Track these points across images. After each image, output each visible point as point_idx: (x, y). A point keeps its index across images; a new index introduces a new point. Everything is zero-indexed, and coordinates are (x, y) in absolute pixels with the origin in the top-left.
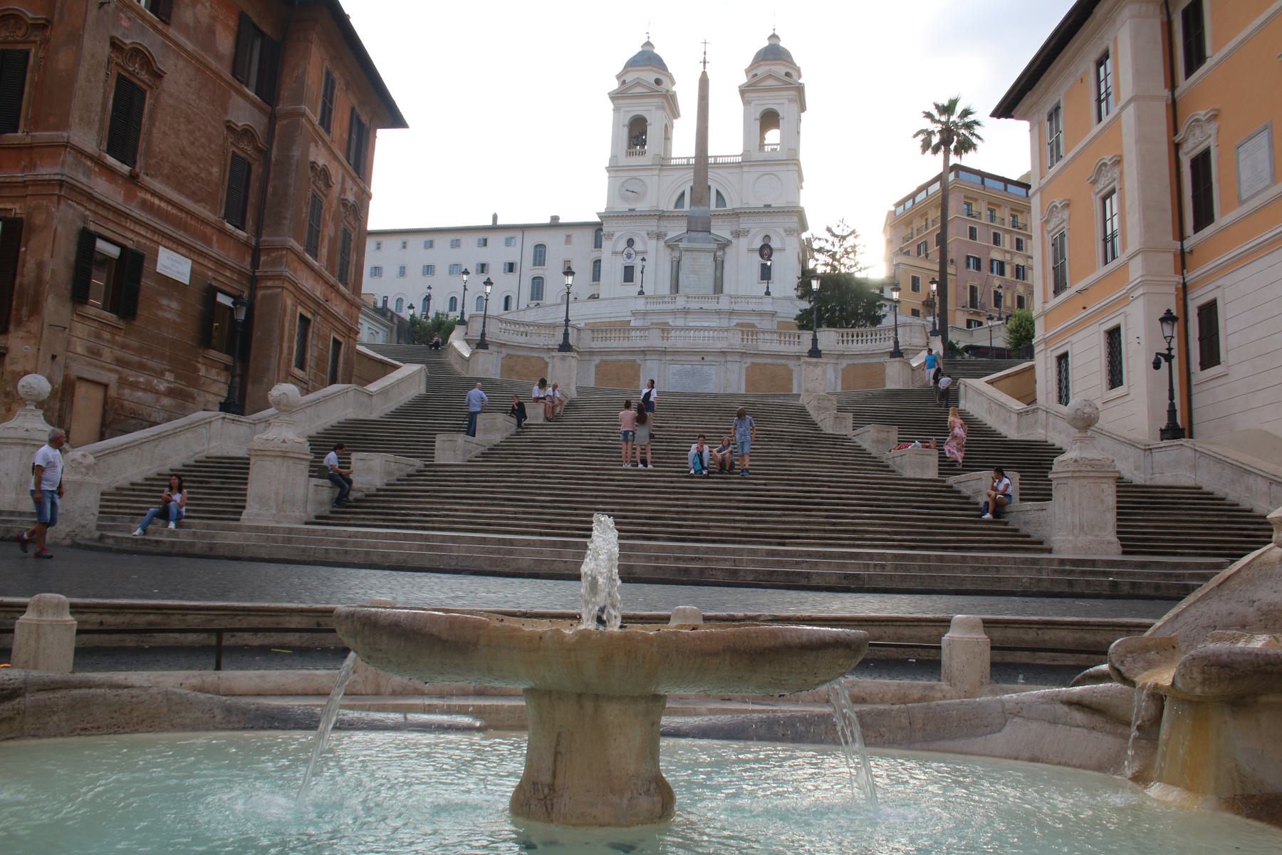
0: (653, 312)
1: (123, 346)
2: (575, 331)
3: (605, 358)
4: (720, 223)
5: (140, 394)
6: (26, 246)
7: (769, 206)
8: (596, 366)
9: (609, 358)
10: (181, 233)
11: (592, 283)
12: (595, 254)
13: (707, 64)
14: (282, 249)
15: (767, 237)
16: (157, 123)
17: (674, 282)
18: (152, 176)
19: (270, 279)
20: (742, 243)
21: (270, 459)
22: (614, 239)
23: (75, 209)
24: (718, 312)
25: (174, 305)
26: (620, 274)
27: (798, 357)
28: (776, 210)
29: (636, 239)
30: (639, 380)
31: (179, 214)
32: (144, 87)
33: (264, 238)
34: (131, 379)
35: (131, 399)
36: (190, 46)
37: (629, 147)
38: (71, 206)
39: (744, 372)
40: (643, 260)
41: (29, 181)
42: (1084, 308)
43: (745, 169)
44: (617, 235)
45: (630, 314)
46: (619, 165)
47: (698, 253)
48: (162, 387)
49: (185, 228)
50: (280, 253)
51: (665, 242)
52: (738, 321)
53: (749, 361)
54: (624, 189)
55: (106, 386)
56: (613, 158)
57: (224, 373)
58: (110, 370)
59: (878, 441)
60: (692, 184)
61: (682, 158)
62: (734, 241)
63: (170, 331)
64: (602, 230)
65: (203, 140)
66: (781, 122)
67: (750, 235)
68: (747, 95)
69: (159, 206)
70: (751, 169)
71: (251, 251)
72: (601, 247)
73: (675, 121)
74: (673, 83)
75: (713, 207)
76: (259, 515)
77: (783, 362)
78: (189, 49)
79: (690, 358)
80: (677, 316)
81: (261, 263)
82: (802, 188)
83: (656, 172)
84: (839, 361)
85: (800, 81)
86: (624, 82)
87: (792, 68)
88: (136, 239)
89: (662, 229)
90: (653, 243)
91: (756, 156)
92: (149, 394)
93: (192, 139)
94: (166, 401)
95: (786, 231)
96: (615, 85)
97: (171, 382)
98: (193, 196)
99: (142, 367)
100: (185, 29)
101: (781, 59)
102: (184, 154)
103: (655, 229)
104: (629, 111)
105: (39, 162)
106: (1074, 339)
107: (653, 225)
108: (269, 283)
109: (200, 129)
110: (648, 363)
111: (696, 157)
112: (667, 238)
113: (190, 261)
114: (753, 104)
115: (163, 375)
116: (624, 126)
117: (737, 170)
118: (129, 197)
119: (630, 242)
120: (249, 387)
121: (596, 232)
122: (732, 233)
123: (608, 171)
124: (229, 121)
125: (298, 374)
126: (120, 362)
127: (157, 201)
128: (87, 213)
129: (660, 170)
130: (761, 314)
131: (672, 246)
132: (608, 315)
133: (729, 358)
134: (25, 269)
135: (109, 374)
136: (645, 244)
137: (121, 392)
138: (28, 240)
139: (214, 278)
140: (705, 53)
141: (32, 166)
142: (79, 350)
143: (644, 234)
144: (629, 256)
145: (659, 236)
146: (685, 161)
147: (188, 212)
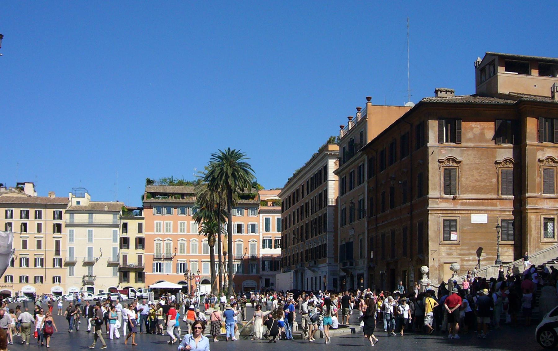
5: (471, 263)
10: (481, 207)
16: (463, 176)
18: (464, 194)
23: (434, 215)
32: (455, 168)
34: (466, 259)
36: (472, 145)
38: (433, 215)
49: (483, 204)
65: (485, 173)
69: (469, 202)
78: (472, 146)
88: (459, 215)
92: (475, 262)
93: (480, 174)
97: (485, 256)
98: (485, 193)
100: (470, 140)
102: (477, 181)
109: (483, 170)
113: (487, 215)
118: (454, 205)
124: (496, 161)
125: (547, 240)
126: (460, 255)
127: (468, 201)
128: (440, 214)
135: (457, 259)
137: (462, 263)
142: (443, 255)
147: (482, 199)
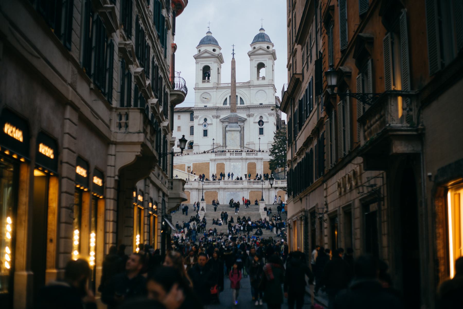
0: (218, 159)
2: (198, 183)
3: (207, 190)
4: (242, 111)
9: (208, 190)
12: (191, 124)
13: (234, 54)
15: (261, 117)
17: (224, 136)
22: (199, 118)
24: (242, 159)
26: (202, 133)
28: (265, 106)
29: (208, 119)
30: (218, 197)
37: (203, 80)
39: (248, 194)
40: (213, 139)
43: (252, 88)
44: (200, 117)
45: (209, 160)
46: (200, 87)
47: (233, 132)
51: (220, 120)
52: (249, 162)
54: (202, 97)
56: (197, 84)
60: (230, 95)
61: (225, 84)
62: (248, 119)
64: (193, 115)
67: (254, 116)
68: (251, 57)
70: (254, 88)
72: (193, 120)
73: (222, 64)
74: (220, 49)
75: (239, 105)
79: (232, 190)
82: (276, 92)
83: (215, 90)
85: (273, 48)
87: (269, 44)
89: (218, 114)
90: (215, 120)
91: (256, 82)
95: (269, 114)
96: (196, 52)
101: (265, 41)
103: (215, 114)
104: (203, 64)
107: (214, 113)
110: (220, 192)
111: (231, 84)
112: (220, 118)
114: (254, 60)
116: (201, 70)
117: (248, 89)
119: (205, 120)
121: (191, 114)
122: (247, 115)
123: (195, 90)
129: (217, 89)
130: (257, 159)
131: (223, 121)
132: (201, 160)
133: (244, 190)
140: (233, 50)
143: (211, 116)
144: (205, 126)
145: (217, 117)
146: (226, 85)
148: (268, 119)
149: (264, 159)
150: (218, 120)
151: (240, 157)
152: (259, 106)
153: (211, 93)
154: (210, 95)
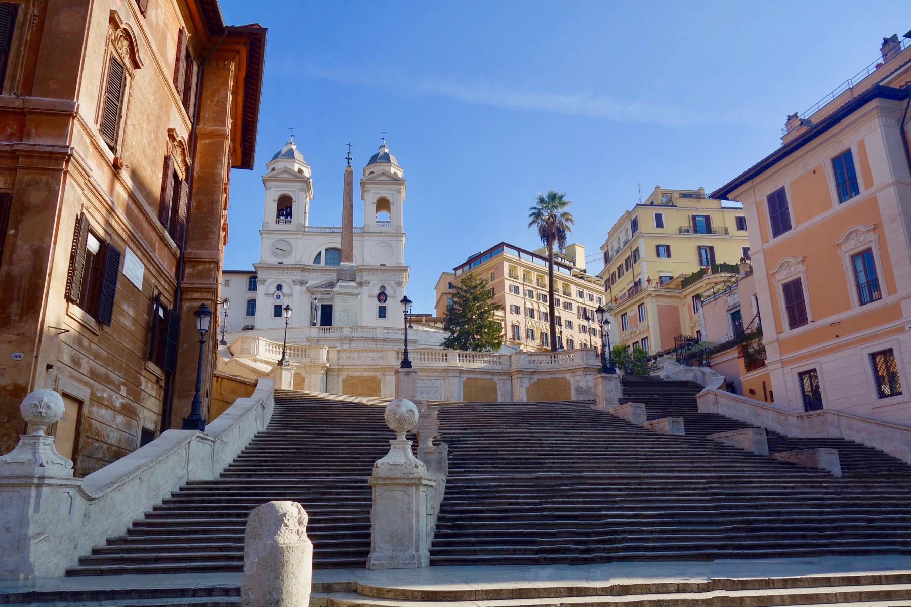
1: (97, 356)
5: (103, 411)
6: (16, 228)
7: (384, 265)
8: (344, 381)
11: (246, 317)
12: (251, 295)
14: (210, 262)
15: (383, 287)
19: (197, 292)
20: (365, 290)
21: (402, 488)
22: (267, 284)
25: (131, 312)
27: (500, 374)
31: (139, 215)
33: (189, 250)
34: (99, 395)
35: (97, 418)
39: (462, 384)
41: (20, 151)
42: (837, 336)
44: (269, 281)
47: (347, 296)
48: (118, 402)
50: (207, 266)
53: (465, 377)
55: (80, 403)
57: (156, 387)
58: (86, 384)
59: (756, 442)
63: (127, 340)
64: (256, 277)
66: (391, 206)
67: (370, 285)
71: (175, 263)
76: (392, 559)
77: (490, 377)
80: (344, 342)
81: (186, 275)
84: (533, 376)
86: (274, 169)
89: (305, 279)
90: (297, 289)
92: (110, 411)
94: (120, 419)
95: (396, 283)
99: (107, 381)
105: (34, 131)
106: (823, 359)
107: (298, 275)
108: (196, 295)
112: (307, 285)
113: (143, 266)
115: (120, 389)
116: (274, 201)
119: (280, 287)
120: (175, 401)
121: (250, 278)
123: (261, 234)
126: (94, 375)
134: (14, 256)
136: (291, 289)
137: (90, 409)
138: (19, 222)
139: (156, 287)
140: (349, 153)
141: (22, 133)
144: (278, 297)
145: (302, 283)
148: (395, 292)
149: (421, 343)
150: (304, 288)
151: (372, 336)
152: (379, 268)
153: (292, 242)
154: (290, 245)
